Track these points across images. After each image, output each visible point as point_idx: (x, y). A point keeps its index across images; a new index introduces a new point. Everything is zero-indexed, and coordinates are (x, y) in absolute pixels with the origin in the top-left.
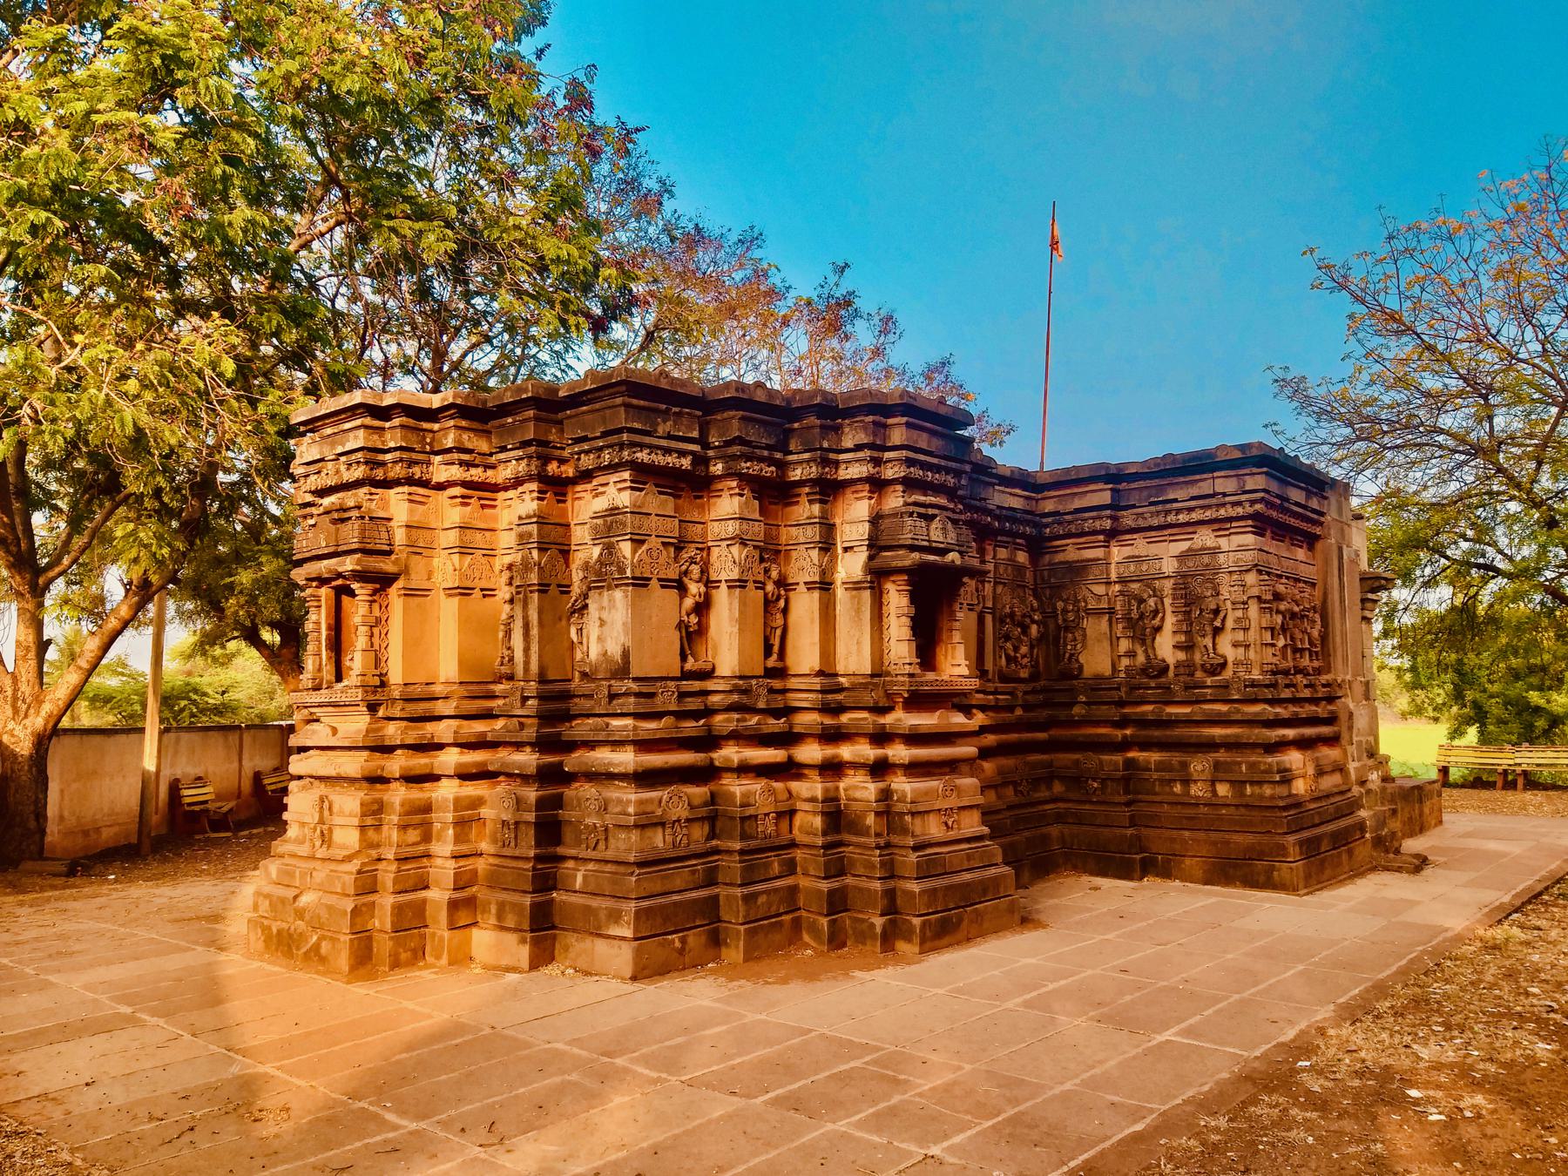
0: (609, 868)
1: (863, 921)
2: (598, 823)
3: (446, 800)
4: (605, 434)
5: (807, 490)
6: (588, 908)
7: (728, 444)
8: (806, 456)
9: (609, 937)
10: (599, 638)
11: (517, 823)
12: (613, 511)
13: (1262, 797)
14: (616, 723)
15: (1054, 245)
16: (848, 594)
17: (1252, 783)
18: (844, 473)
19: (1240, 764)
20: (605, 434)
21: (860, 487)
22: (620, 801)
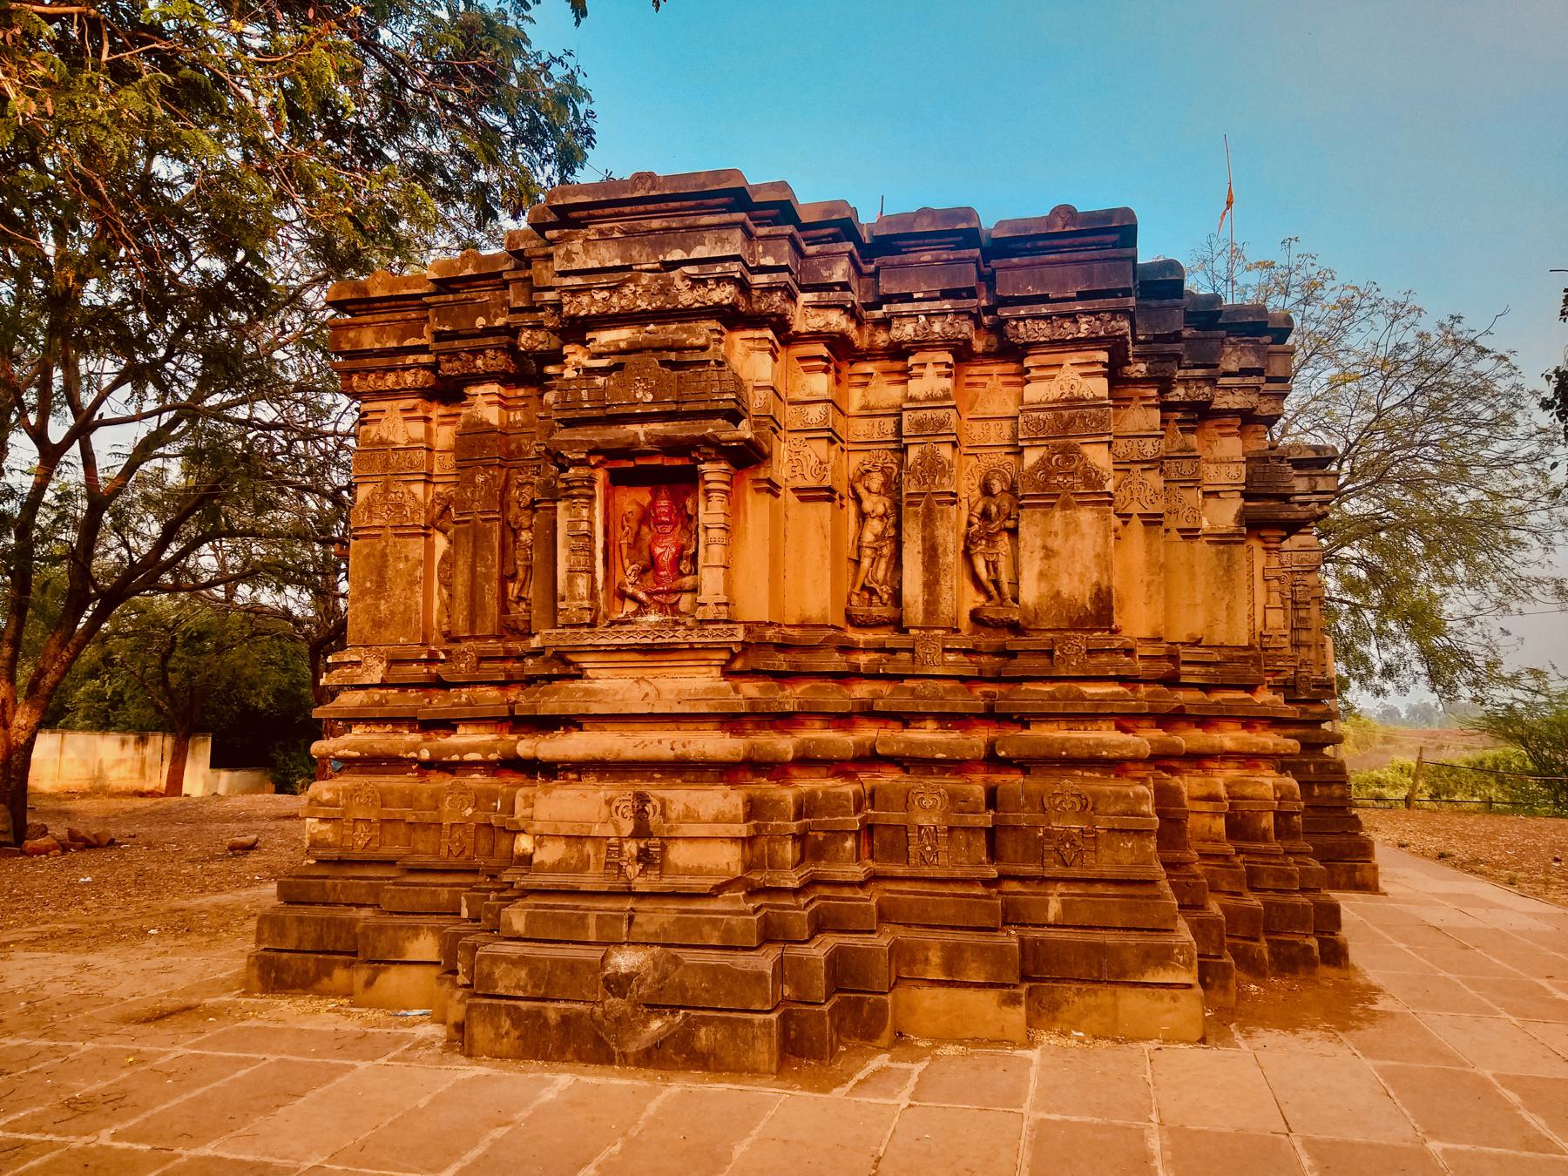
0: (1099, 889)
1: (1294, 943)
2: (1075, 827)
3: (847, 795)
4: (1082, 296)
5: (1179, 416)
6: (1101, 949)
7: (1158, 339)
8: (1199, 372)
9: (1136, 984)
10: (1042, 575)
11: (951, 829)
12: (1074, 402)
13: (1331, 798)
14: (1090, 689)
15: (1229, 203)
16: (1213, 549)
17: (1320, 784)
18: (1223, 401)
19: (1307, 764)
20: (1082, 296)
21: (1228, 421)
22: (1120, 797)
